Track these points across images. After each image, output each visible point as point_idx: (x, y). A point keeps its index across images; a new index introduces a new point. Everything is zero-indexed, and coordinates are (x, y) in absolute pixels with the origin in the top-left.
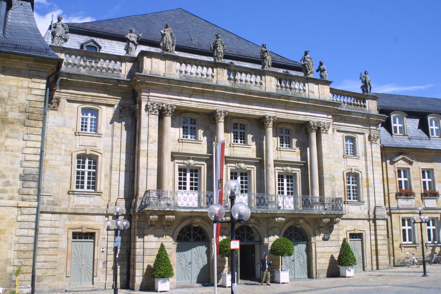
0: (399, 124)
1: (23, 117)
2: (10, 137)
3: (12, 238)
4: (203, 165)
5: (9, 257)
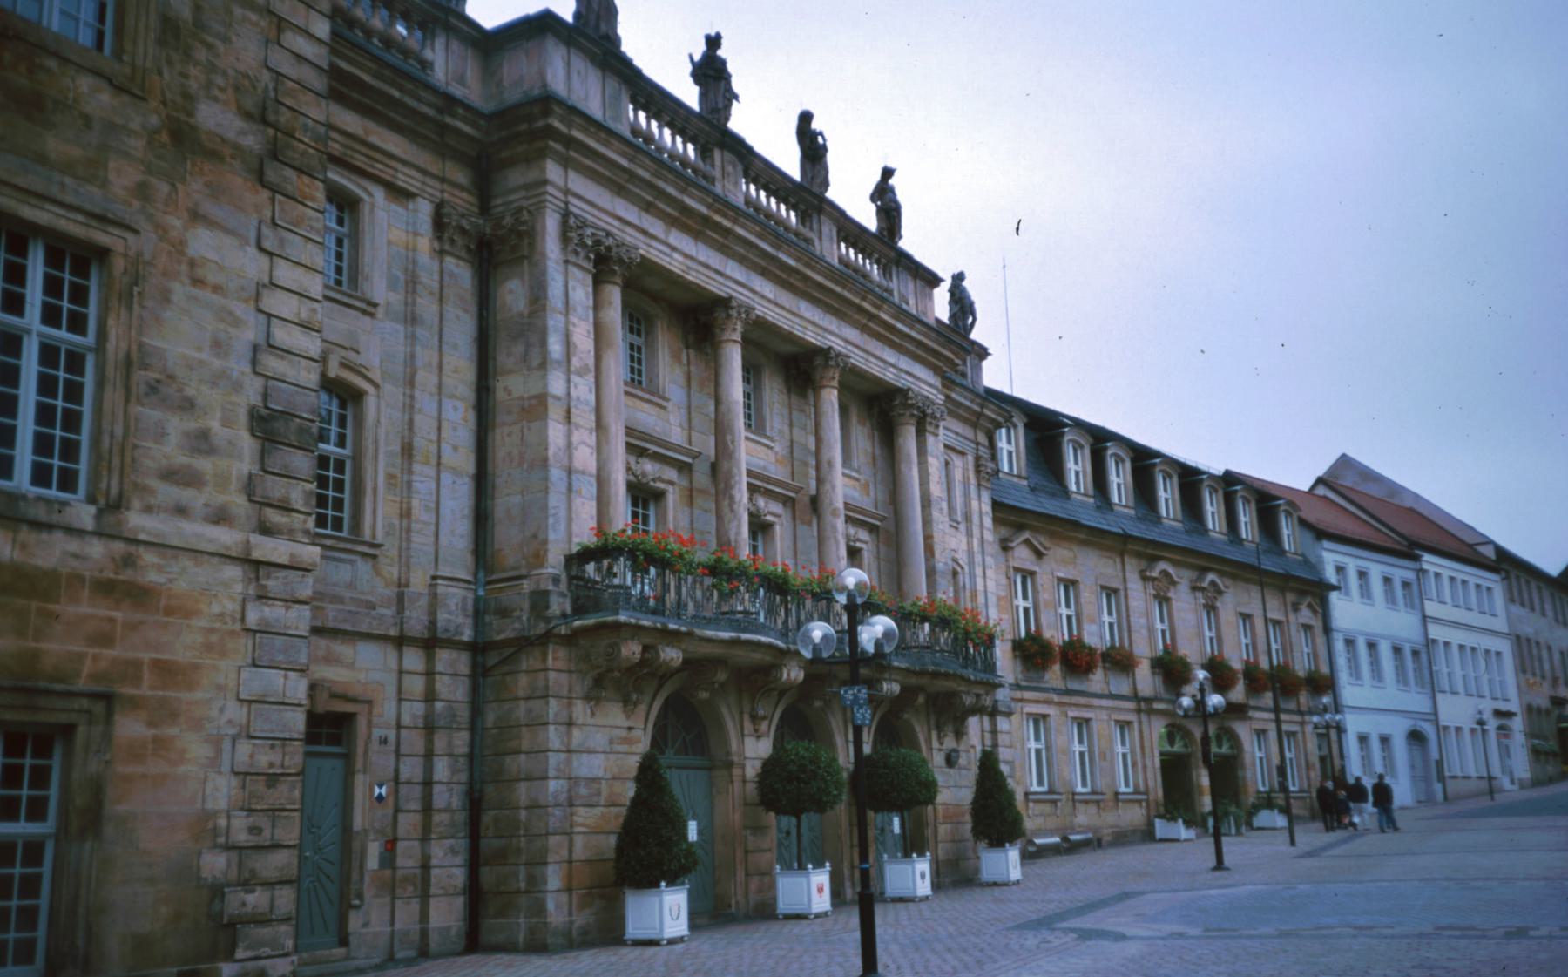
2: (211, 224)
3: (222, 710)
4: (671, 483)
5: (209, 805)
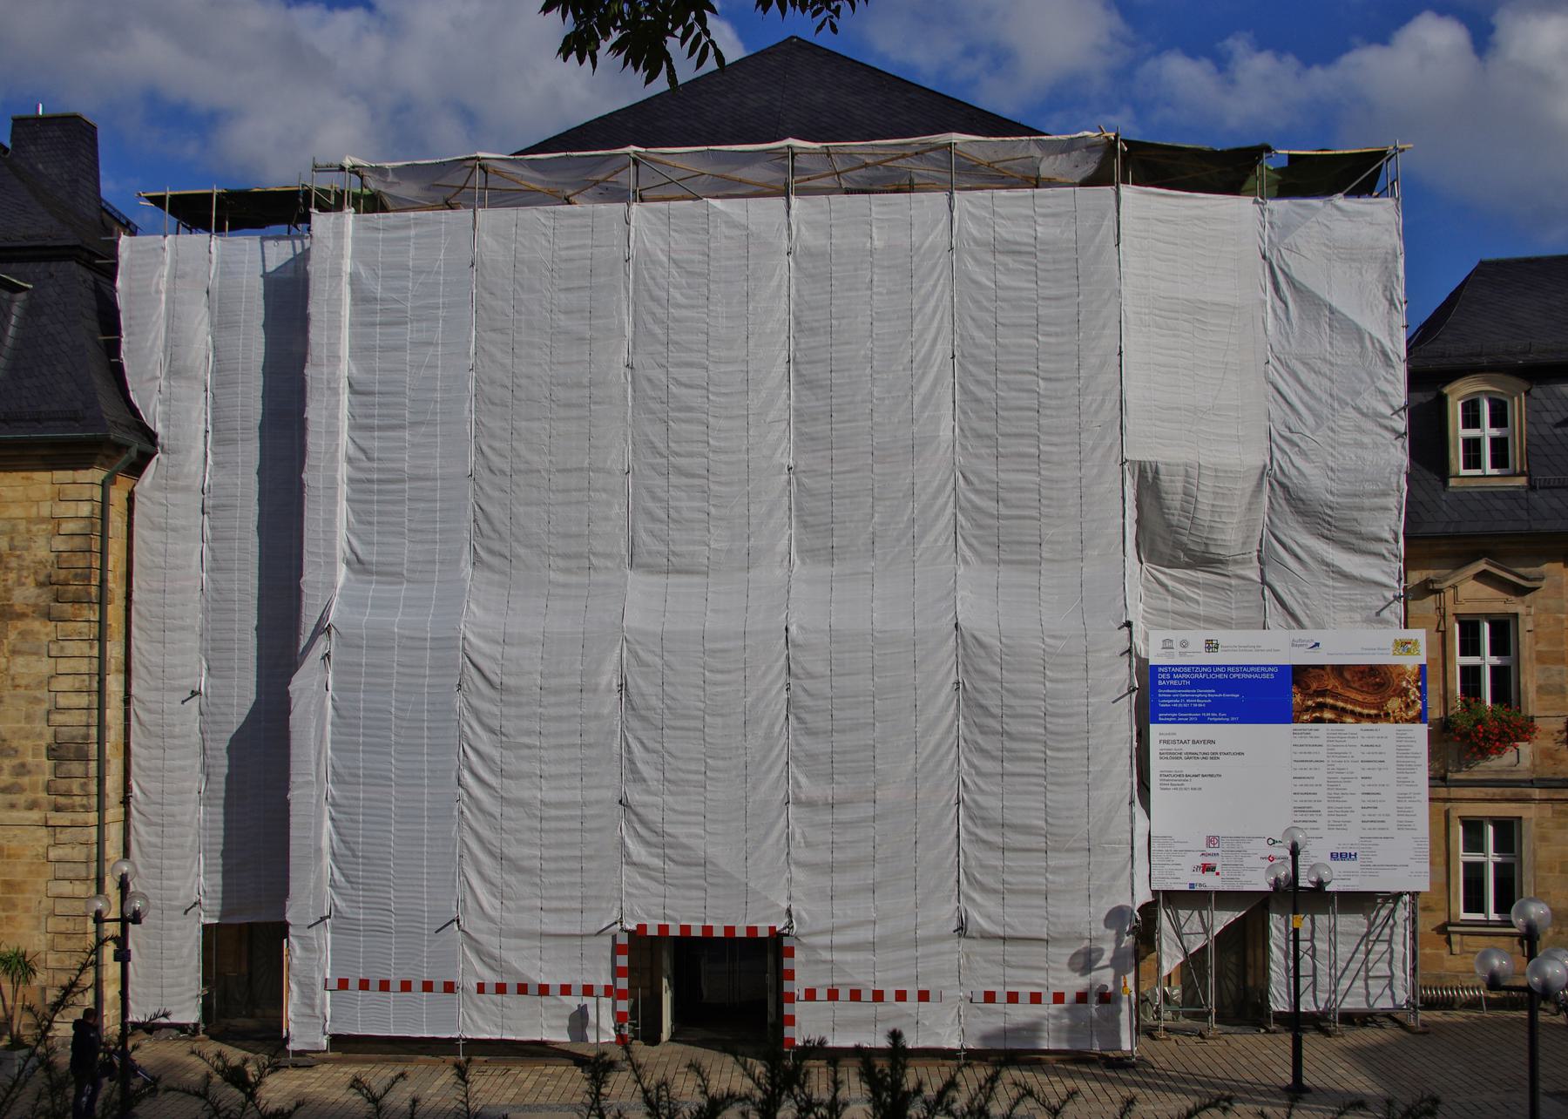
0: (1492, 425)
1: (44, 597)
